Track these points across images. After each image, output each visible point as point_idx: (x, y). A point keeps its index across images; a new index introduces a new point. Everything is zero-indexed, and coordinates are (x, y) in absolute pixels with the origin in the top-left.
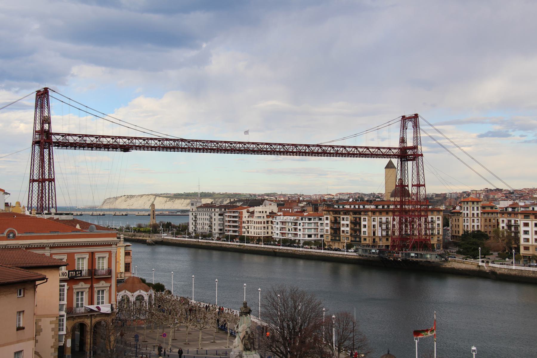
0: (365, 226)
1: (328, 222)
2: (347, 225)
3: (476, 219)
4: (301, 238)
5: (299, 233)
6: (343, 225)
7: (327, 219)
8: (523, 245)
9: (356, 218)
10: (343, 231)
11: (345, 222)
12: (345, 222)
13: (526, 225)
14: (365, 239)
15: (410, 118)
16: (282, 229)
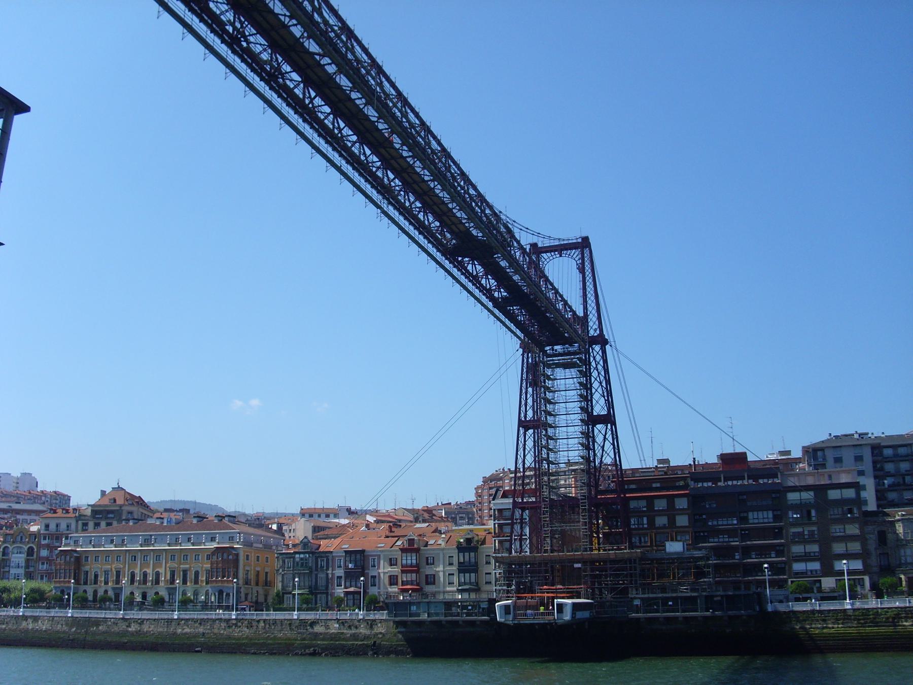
15: (561, 249)
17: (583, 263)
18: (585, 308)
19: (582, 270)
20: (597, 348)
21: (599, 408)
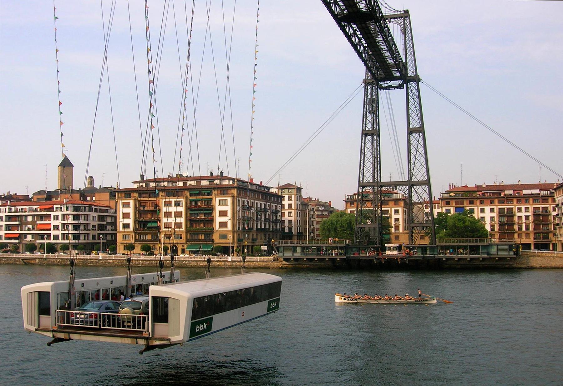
0: (223, 214)
1: (130, 210)
2: (178, 215)
3: (286, 213)
4: (60, 241)
5: (53, 233)
6: (168, 214)
7: (126, 205)
10: (167, 225)
11: (172, 209)
12: (172, 209)
14: (225, 237)
16: (8, 227)
17: (405, 28)
18: (406, 58)
19: (404, 32)
20: (413, 84)
21: (415, 124)
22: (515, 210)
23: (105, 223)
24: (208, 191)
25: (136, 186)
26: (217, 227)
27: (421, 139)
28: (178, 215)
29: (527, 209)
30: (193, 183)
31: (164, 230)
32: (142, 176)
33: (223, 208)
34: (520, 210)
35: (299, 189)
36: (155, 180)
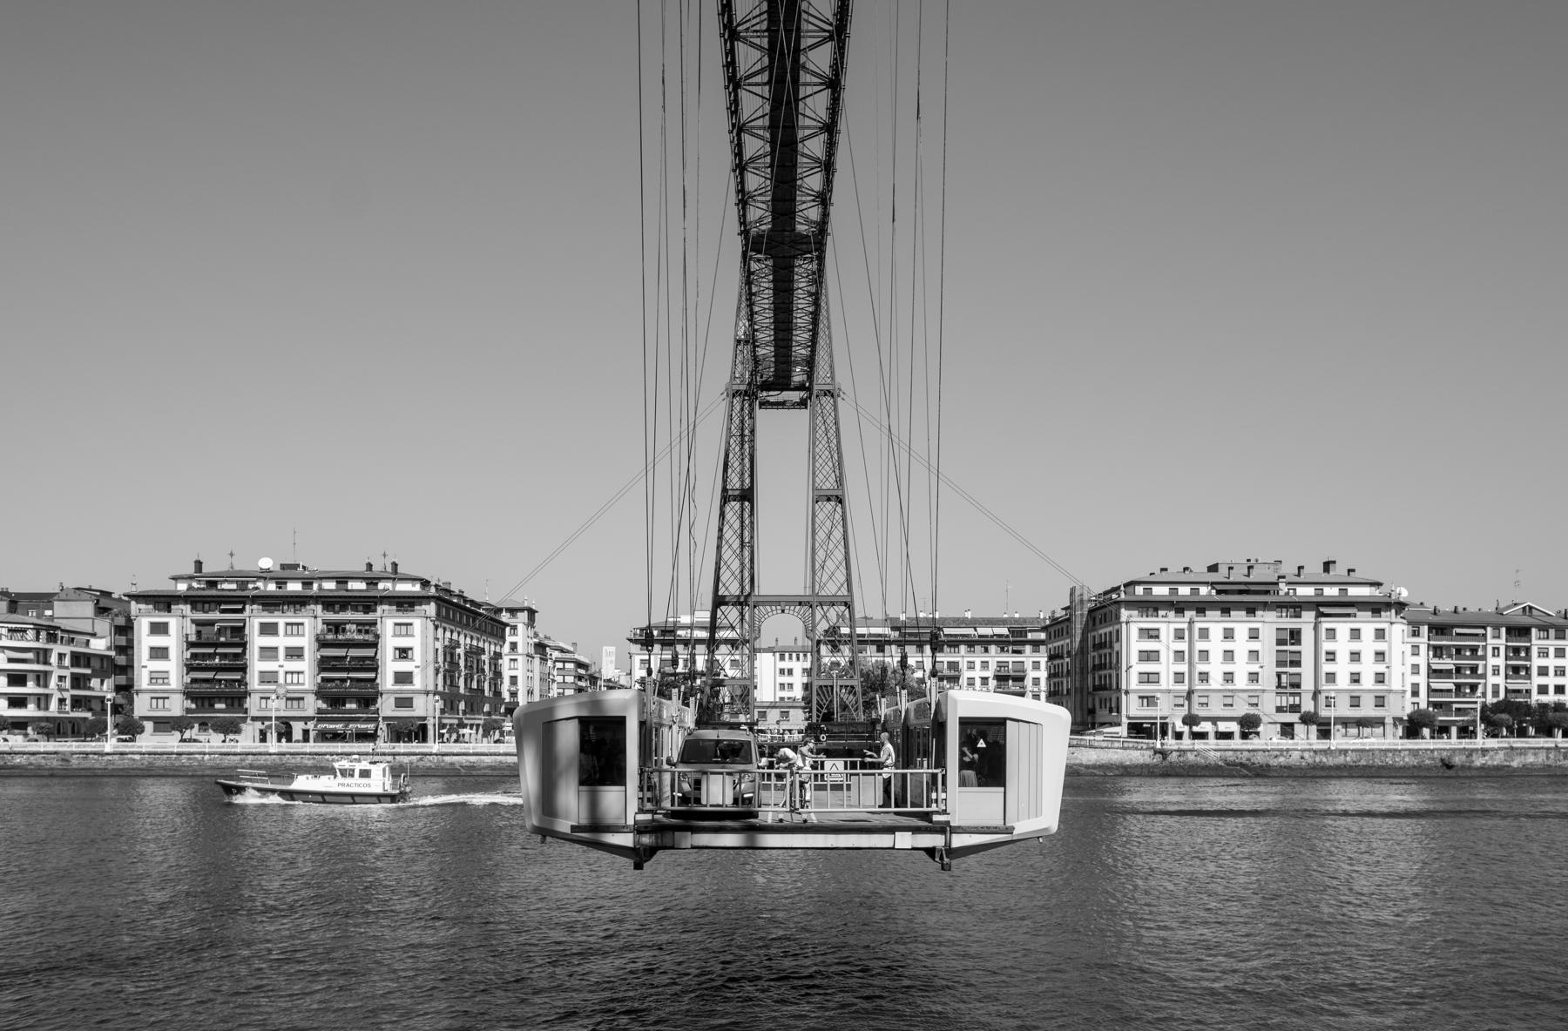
1: (172, 641)
2: (295, 653)
8: (1136, 691)
9: (337, 627)
10: (268, 678)
11: (281, 641)
12: (281, 641)
13: (1152, 634)
21: (829, 485)
22: (963, 665)
23: (88, 671)
24: (368, 603)
25: (182, 587)
26: (387, 681)
27: (838, 516)
28: (295, 653)
29: (985, 665)
30: (330, 585)
31: (257, 686)
32: (199, 564)
33: (404, 642)
34: (971, 666)
35: (532, 613)
36: (228, 577)
